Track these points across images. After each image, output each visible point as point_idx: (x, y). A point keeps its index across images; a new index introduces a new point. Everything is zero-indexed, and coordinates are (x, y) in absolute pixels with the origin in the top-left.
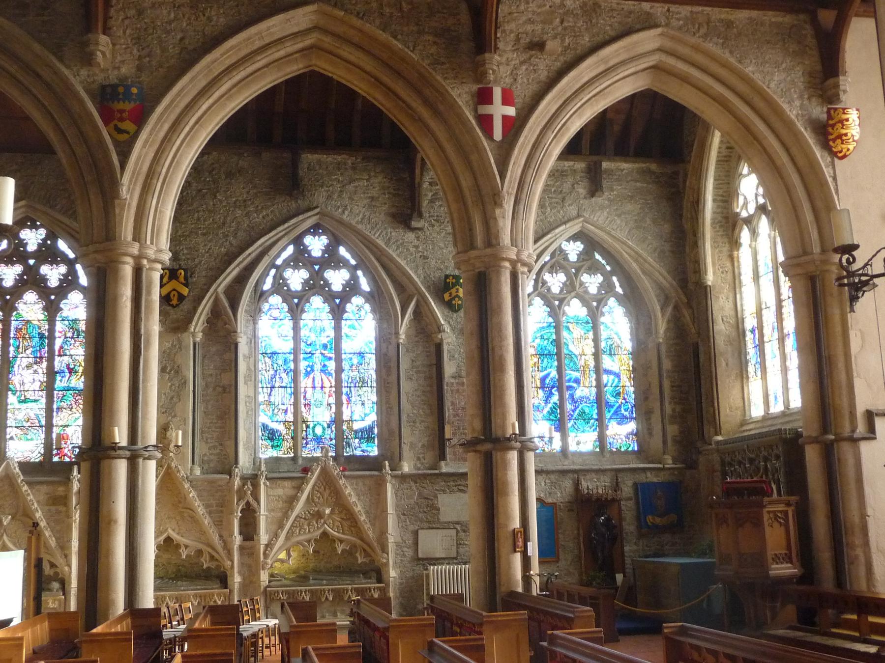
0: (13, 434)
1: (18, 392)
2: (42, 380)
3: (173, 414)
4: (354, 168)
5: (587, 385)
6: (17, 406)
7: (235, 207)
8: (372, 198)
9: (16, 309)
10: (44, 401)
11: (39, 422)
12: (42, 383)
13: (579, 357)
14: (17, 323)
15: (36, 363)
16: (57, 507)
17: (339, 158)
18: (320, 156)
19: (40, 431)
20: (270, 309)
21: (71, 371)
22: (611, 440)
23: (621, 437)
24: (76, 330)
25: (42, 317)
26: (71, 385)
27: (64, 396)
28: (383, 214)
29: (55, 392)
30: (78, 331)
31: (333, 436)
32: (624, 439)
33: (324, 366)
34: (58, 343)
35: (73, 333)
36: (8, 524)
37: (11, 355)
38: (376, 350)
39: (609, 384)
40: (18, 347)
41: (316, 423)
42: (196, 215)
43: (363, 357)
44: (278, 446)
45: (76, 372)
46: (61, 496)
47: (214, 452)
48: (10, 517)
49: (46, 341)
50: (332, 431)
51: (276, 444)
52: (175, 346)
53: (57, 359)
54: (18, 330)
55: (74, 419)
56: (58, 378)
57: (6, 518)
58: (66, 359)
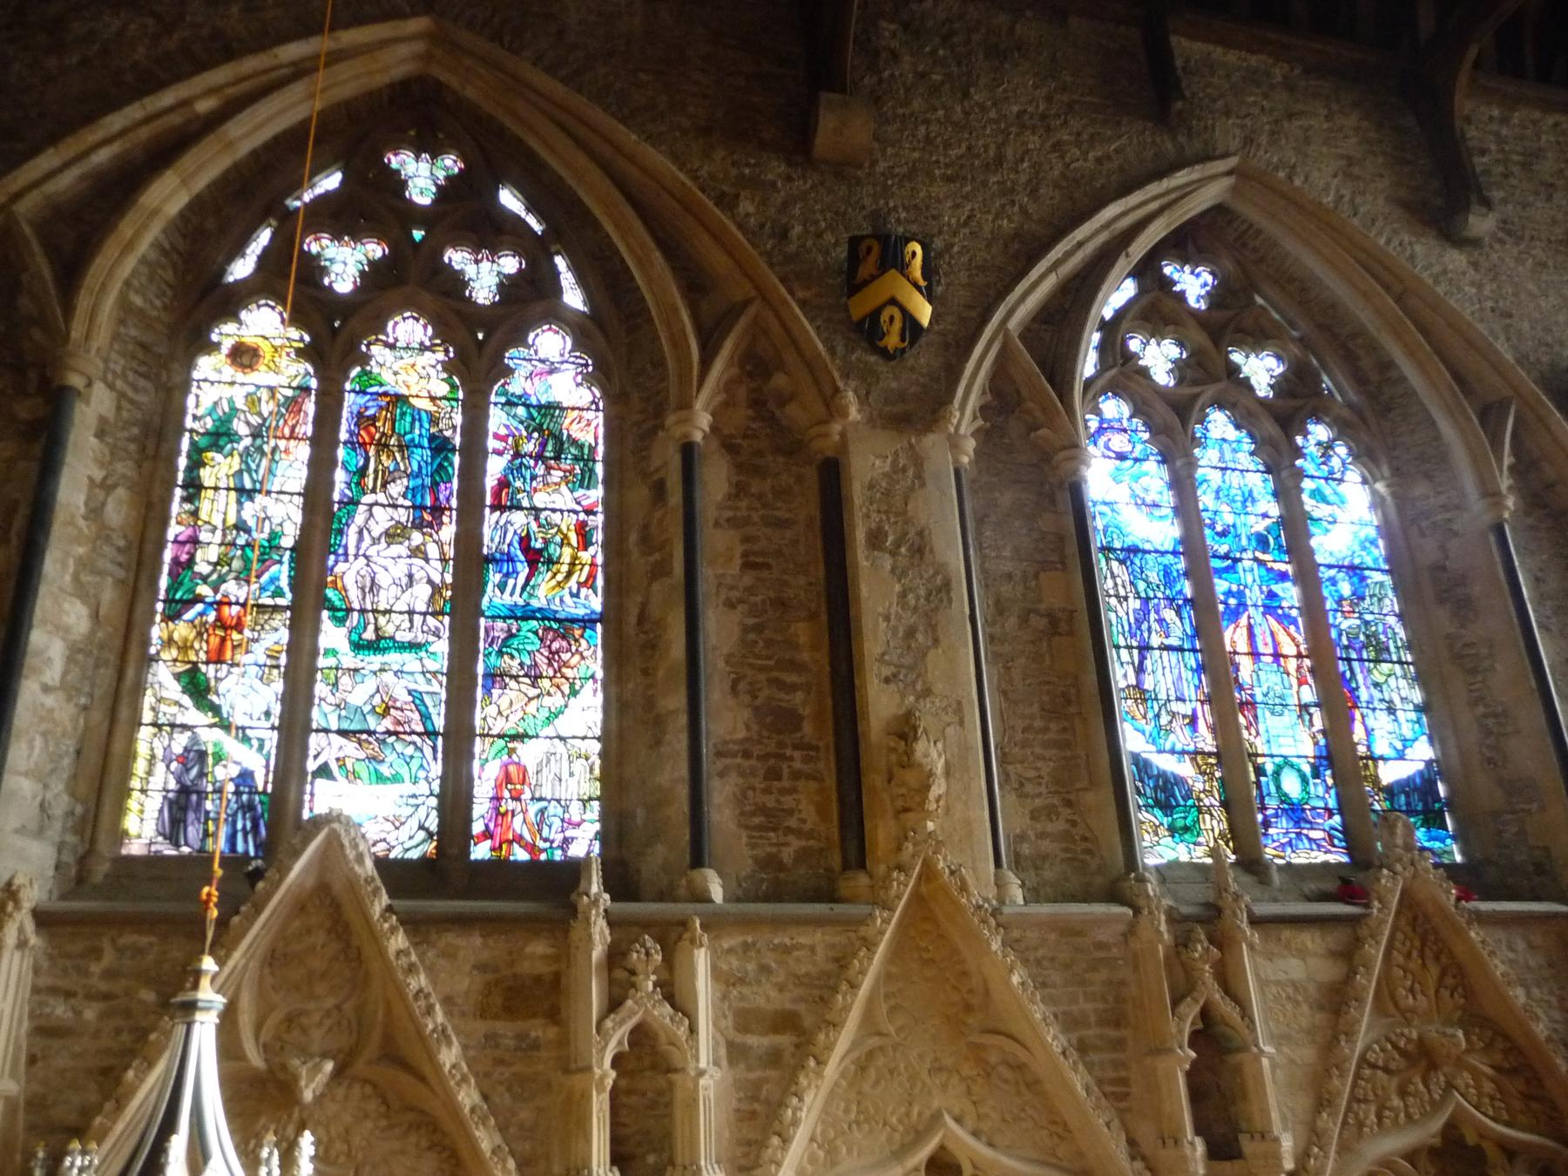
0: (329, 756)
1: (356, 614)
2: (437, 579)
3: (919, 687)
4: (1289, 87)
6: (349, 659)
7: (1023, 127)
8: (1350, 161)
9: (365, 359)
10: (442, 647)
11: (425, 717)
12: (436, 589)
14: (362, 400)
15: (419, 525)
16: (520, 1025)
17: (1253, 60)
18: (1211, 47)
19: (428, 751)
20: (1101, 430)
21: (535, 558)
24: (551, 434)
25: (442, 389)
26: (535, 603)
27: (511, 636)
28: (1381, 201)
29: (482, 621)
30: (558, 438)
31: (1332, 803)
33: (1272, 595)
34: (495, 467)
35: (543, 445)
36: (319, 1099)
37: (336, 497)
38: (1388, 560)
40: (362, 472)
41: (1278, 760)
42: (922, 129)
43: (1363, 579)
44: (1186, 829)
45: (550, 562)
46: (538, 979)
47: (1050, 828)
48: (329, 1066)
49: (456, 460)
50: (1328, 789)
51: (1180, 823)
52: (904, 470)
53: (490, 518)
54: (361, 419)
55: (544, 713)
56: (494, 577)
57: (317, 1069)
58: (519, 519)
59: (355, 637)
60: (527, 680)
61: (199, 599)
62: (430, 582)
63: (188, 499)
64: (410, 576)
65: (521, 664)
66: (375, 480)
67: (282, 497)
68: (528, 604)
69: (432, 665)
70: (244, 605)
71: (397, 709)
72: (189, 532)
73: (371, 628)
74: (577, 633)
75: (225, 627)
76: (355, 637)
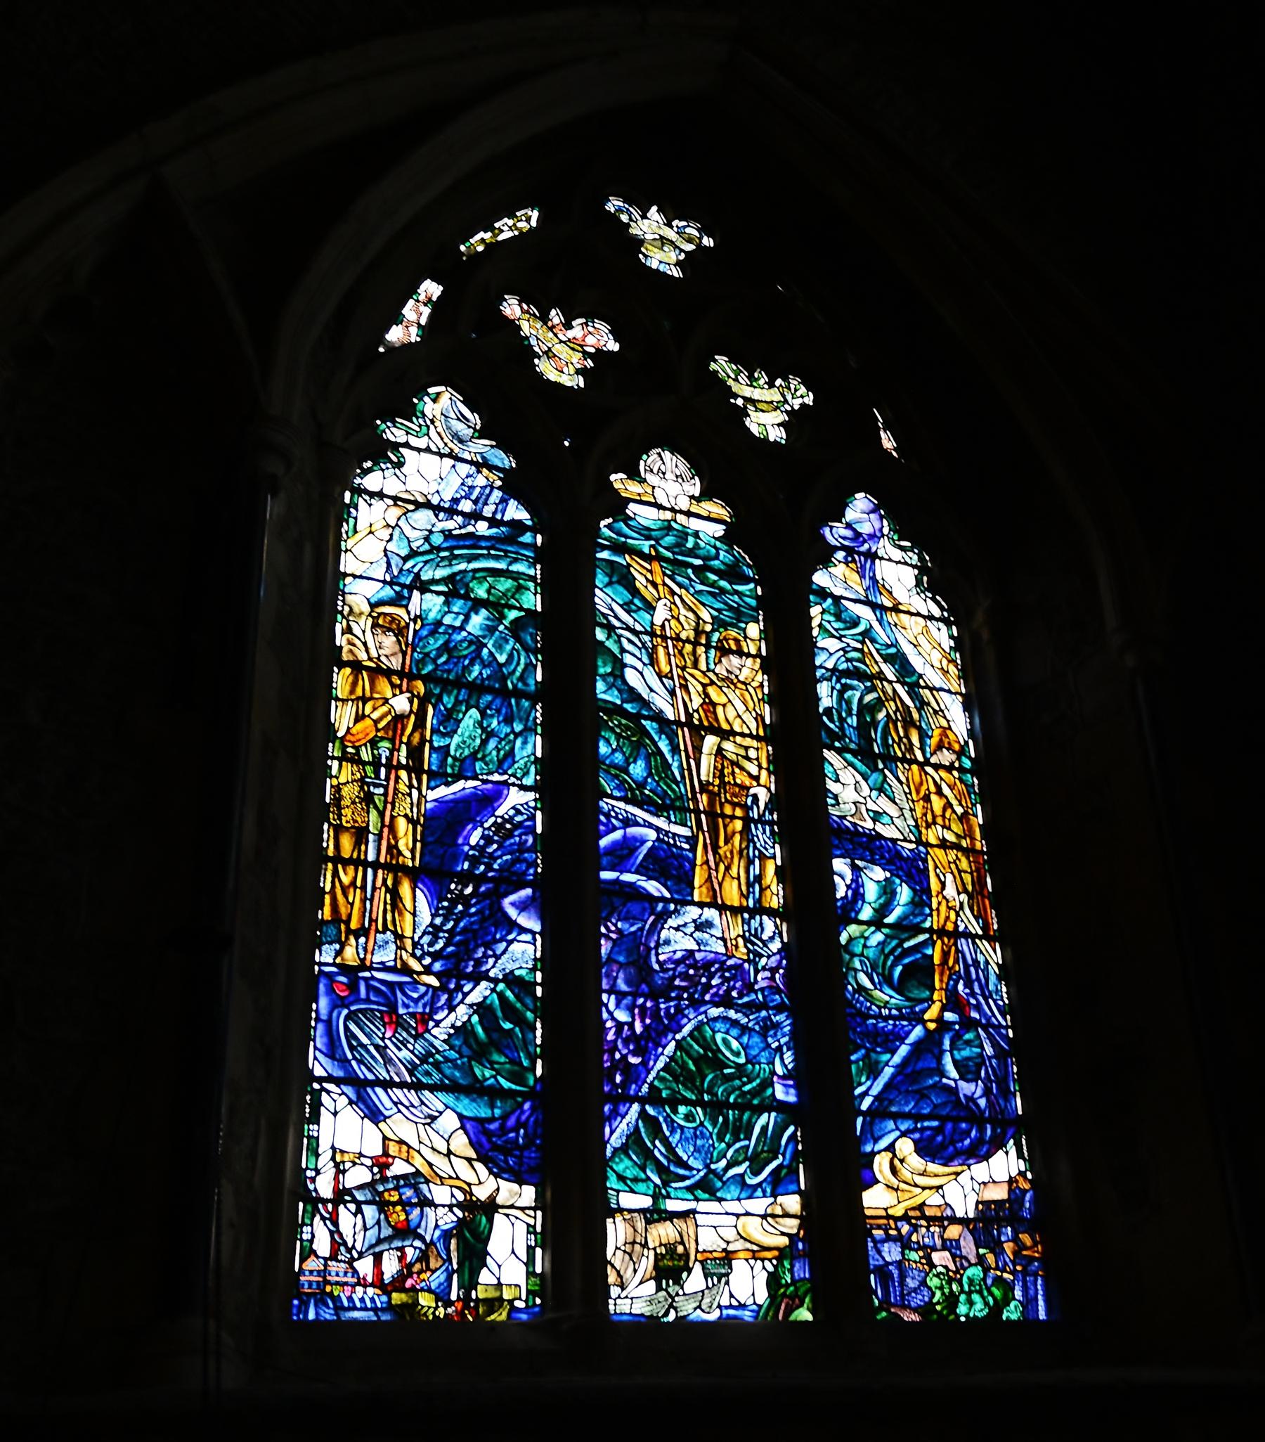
5: (731, 894)
13: (684, 736)
22: (891, 1253)
23: (953, 1231)
32: (968, 1247)
39: (866, 913)
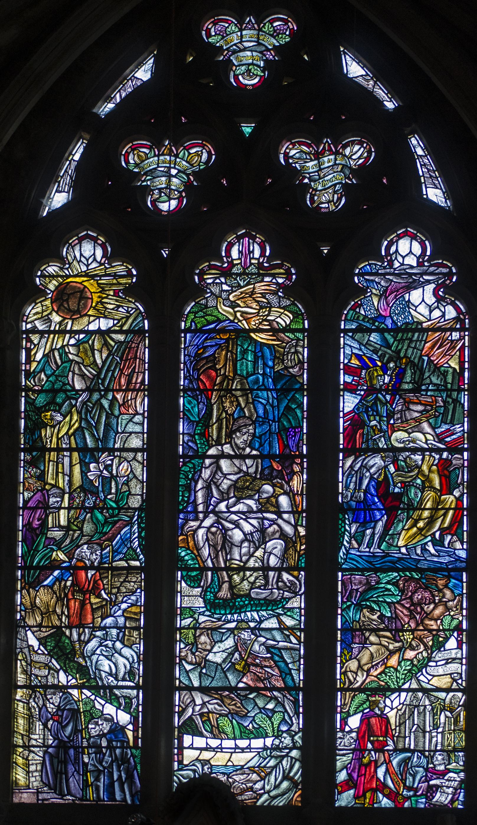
2: (289, 530)
27: (370, 588)
59: (209, 596)
60: (388, 634)
61: (55, 565)
62: (283, 536)
63: (32, 463)
64: (262, 530)
65: (382, 617)
66: (220, 429)
67: (125, 454)
68: (387, 555)
69: (289, 622)
70: (98, 569)
71: (257, 665)
72: (38, 496)
73: (226, 586)
74: (441, 583)
75: (82, 591)
76: (209, 596)
